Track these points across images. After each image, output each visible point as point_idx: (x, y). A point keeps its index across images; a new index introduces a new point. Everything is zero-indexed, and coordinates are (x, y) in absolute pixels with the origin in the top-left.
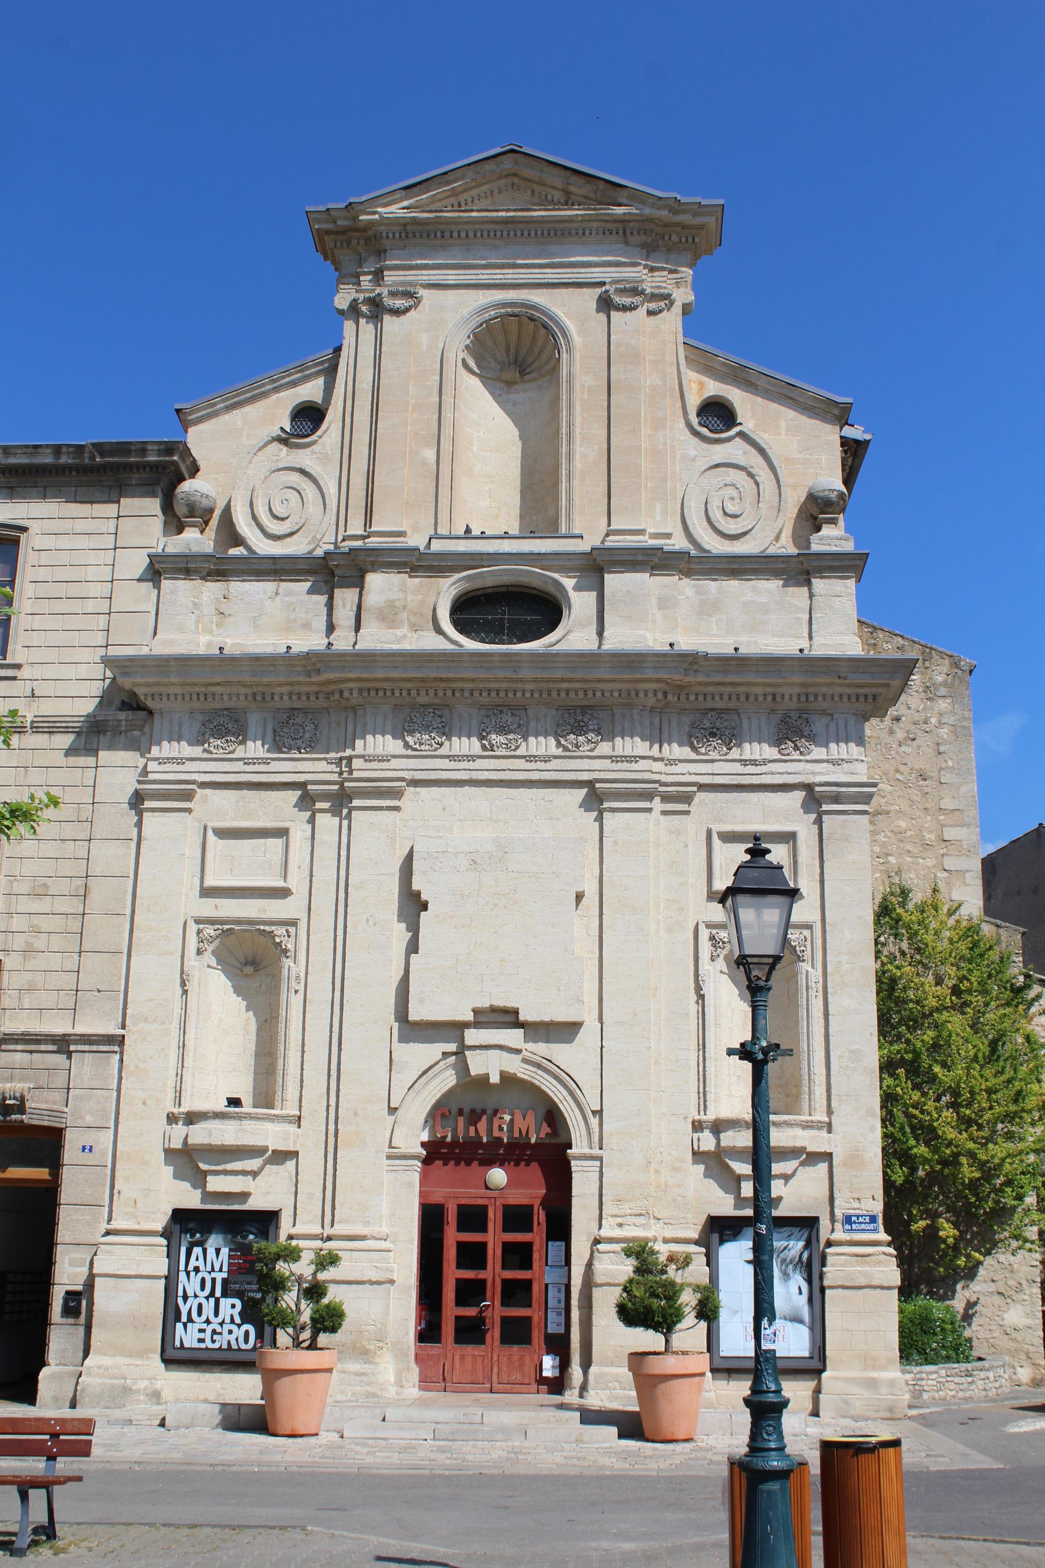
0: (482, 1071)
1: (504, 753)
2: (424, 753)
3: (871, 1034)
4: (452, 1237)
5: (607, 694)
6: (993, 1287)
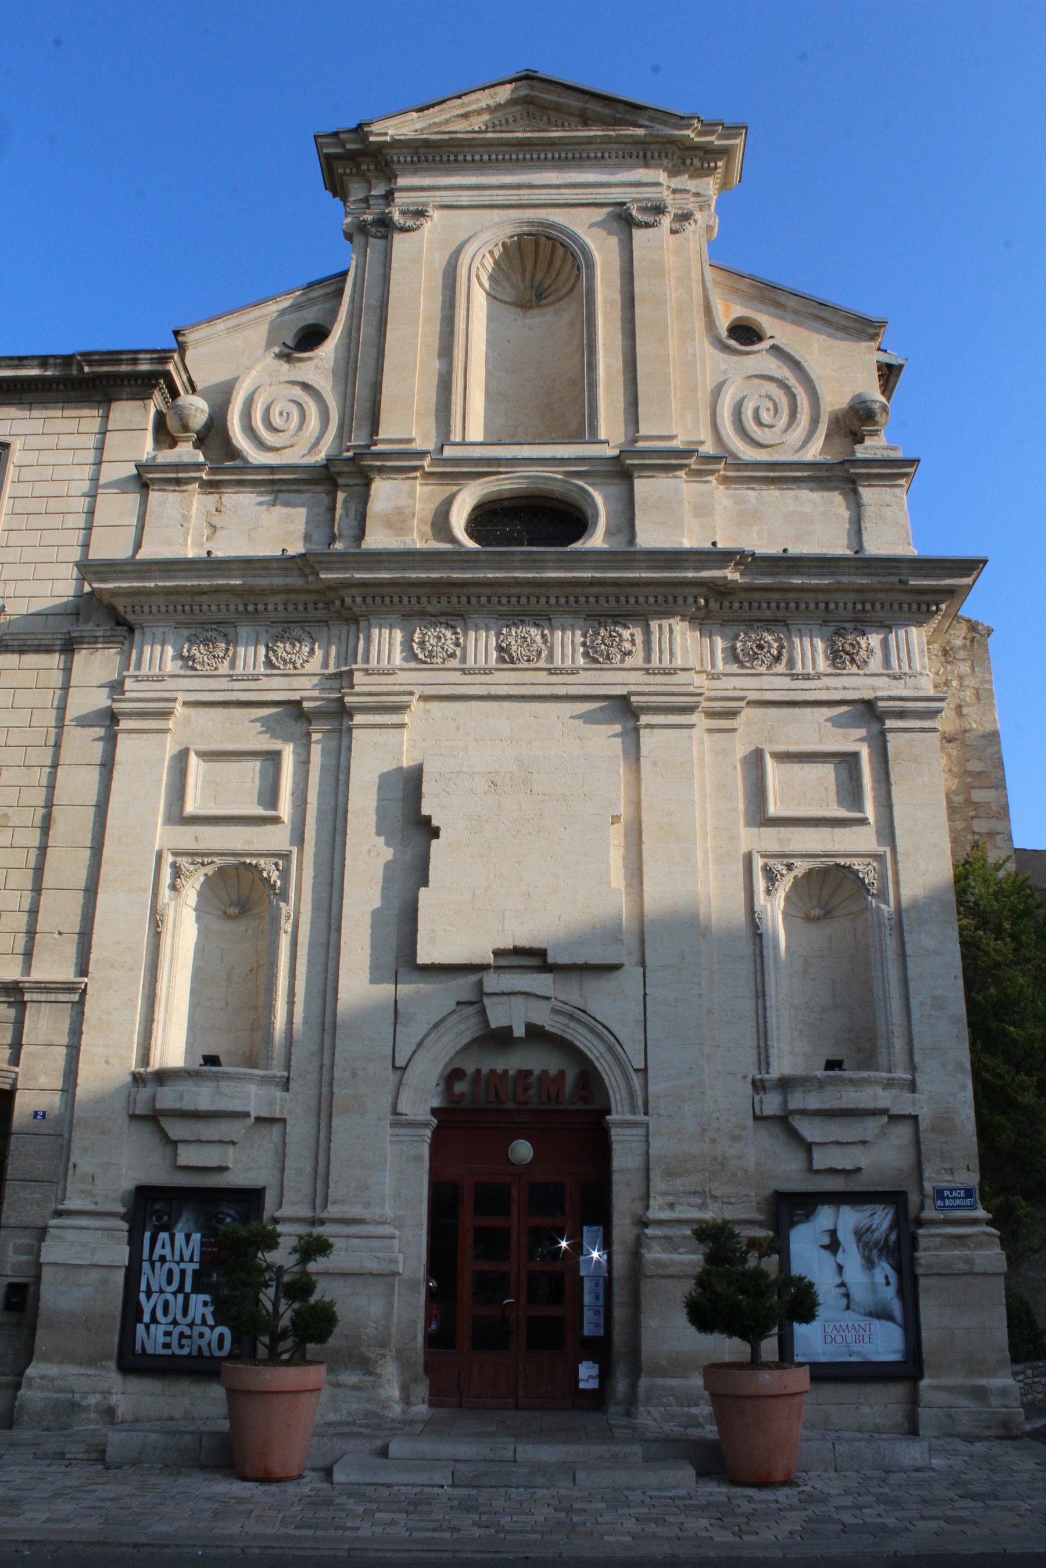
0: (504, 1023)
1: (526, 665)
2: (436, 666)
3: (955, 977)
4: (468, 1220)
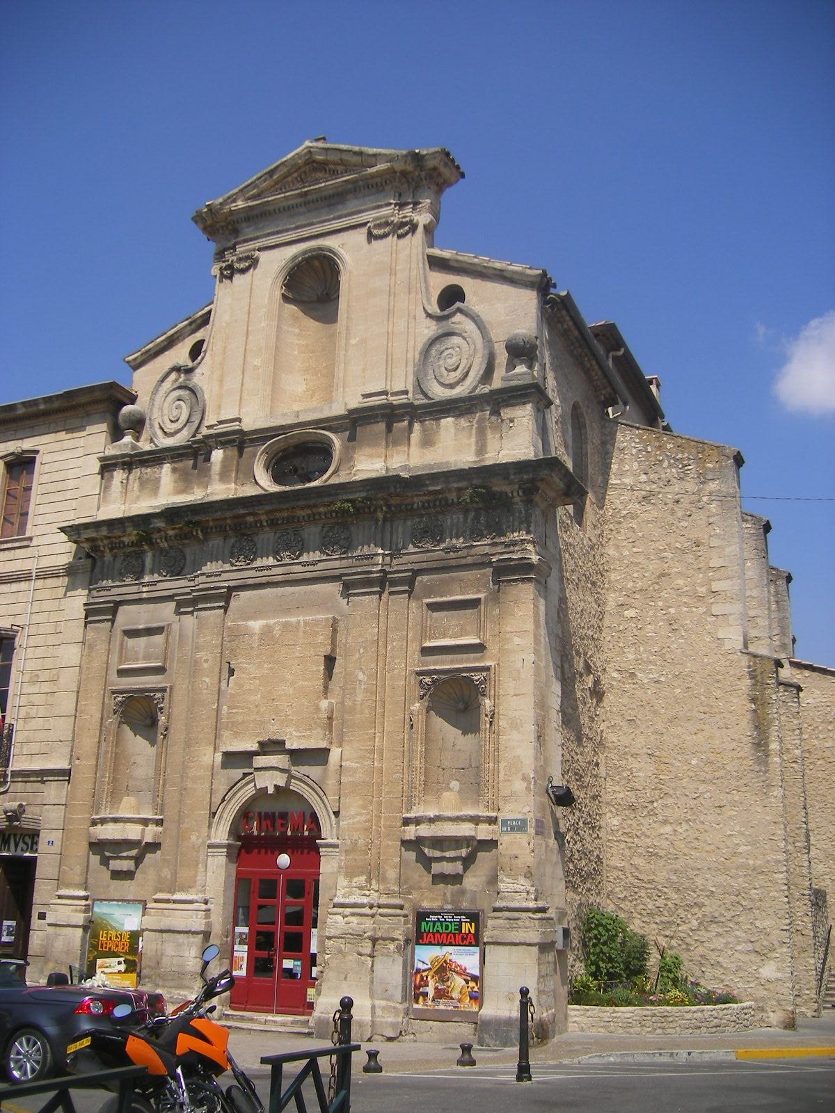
6: (750, 947)
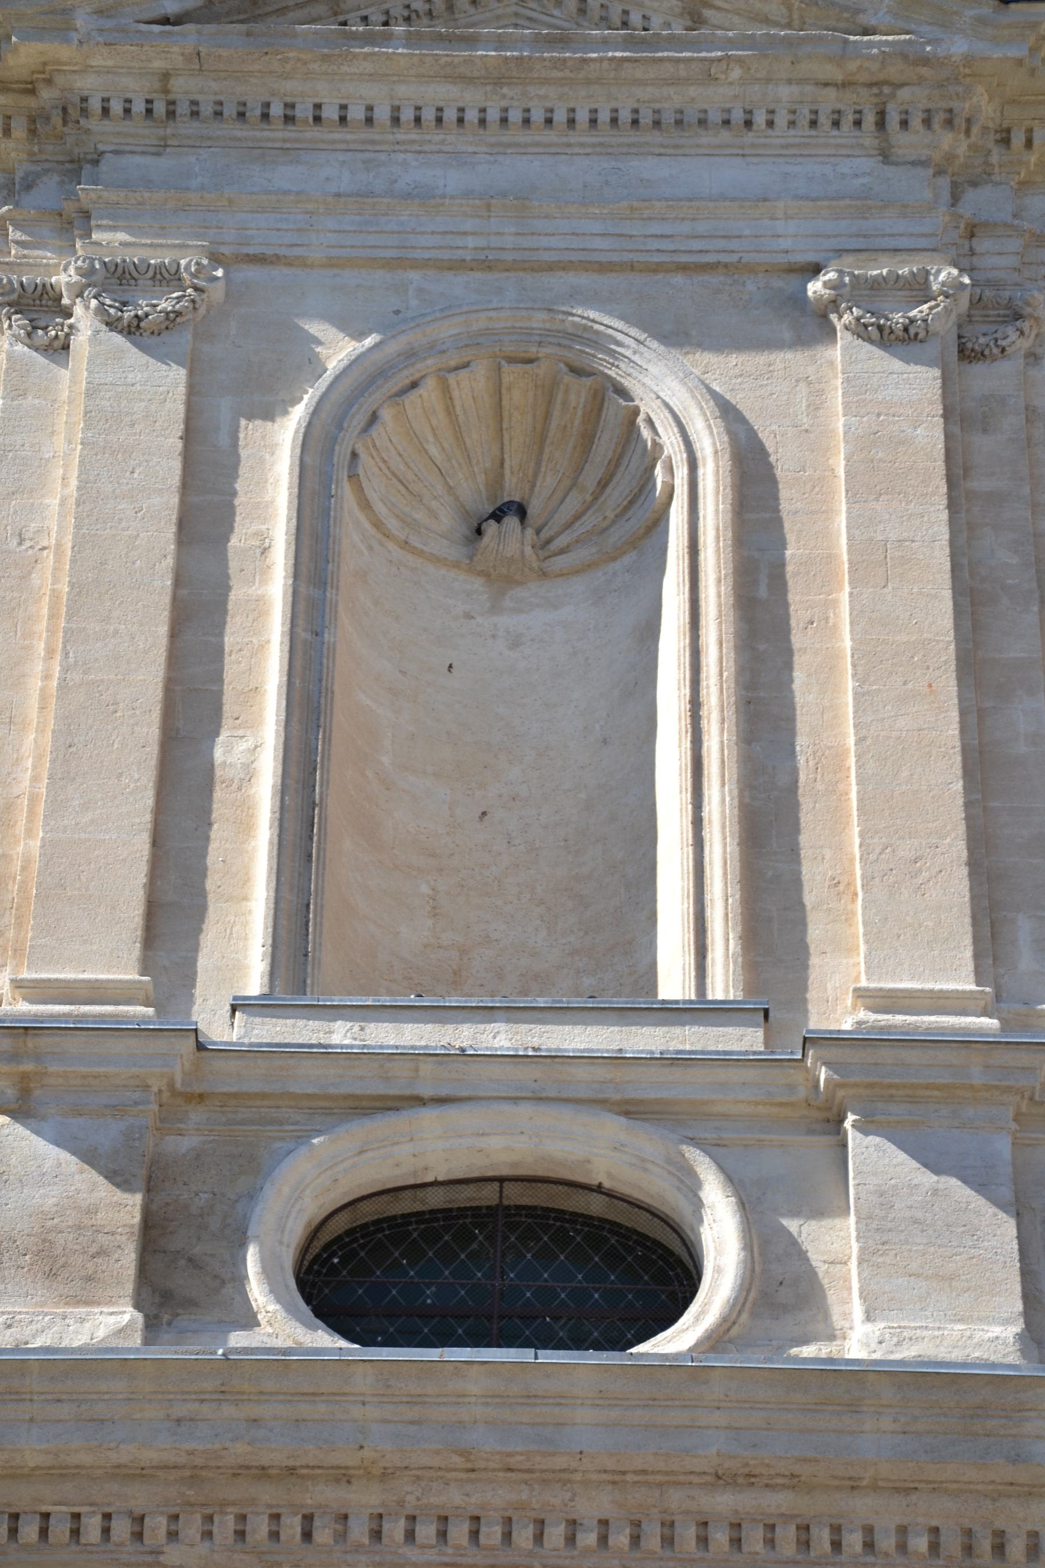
5: (887, 1542)
